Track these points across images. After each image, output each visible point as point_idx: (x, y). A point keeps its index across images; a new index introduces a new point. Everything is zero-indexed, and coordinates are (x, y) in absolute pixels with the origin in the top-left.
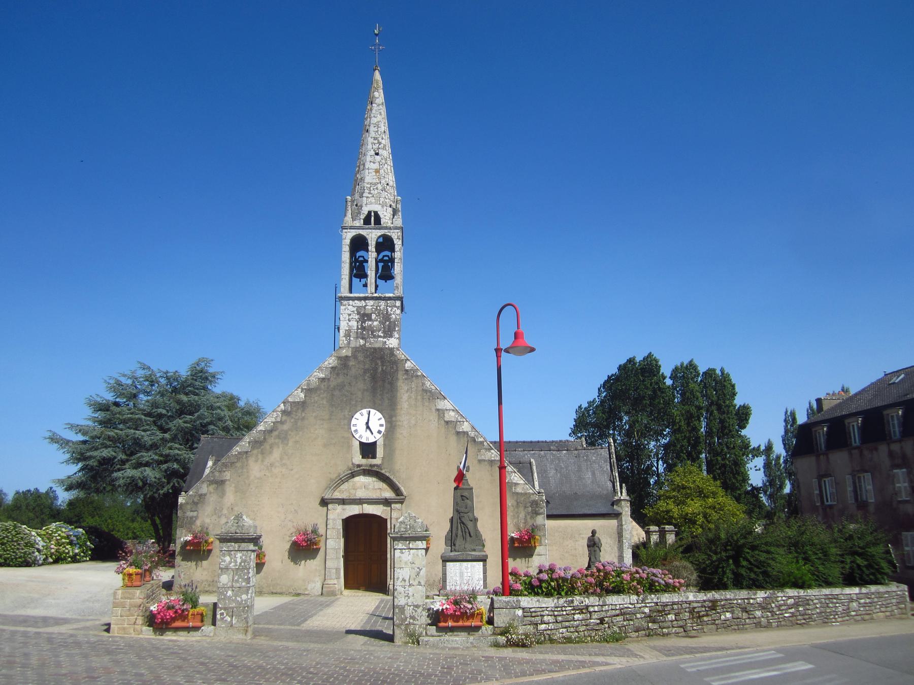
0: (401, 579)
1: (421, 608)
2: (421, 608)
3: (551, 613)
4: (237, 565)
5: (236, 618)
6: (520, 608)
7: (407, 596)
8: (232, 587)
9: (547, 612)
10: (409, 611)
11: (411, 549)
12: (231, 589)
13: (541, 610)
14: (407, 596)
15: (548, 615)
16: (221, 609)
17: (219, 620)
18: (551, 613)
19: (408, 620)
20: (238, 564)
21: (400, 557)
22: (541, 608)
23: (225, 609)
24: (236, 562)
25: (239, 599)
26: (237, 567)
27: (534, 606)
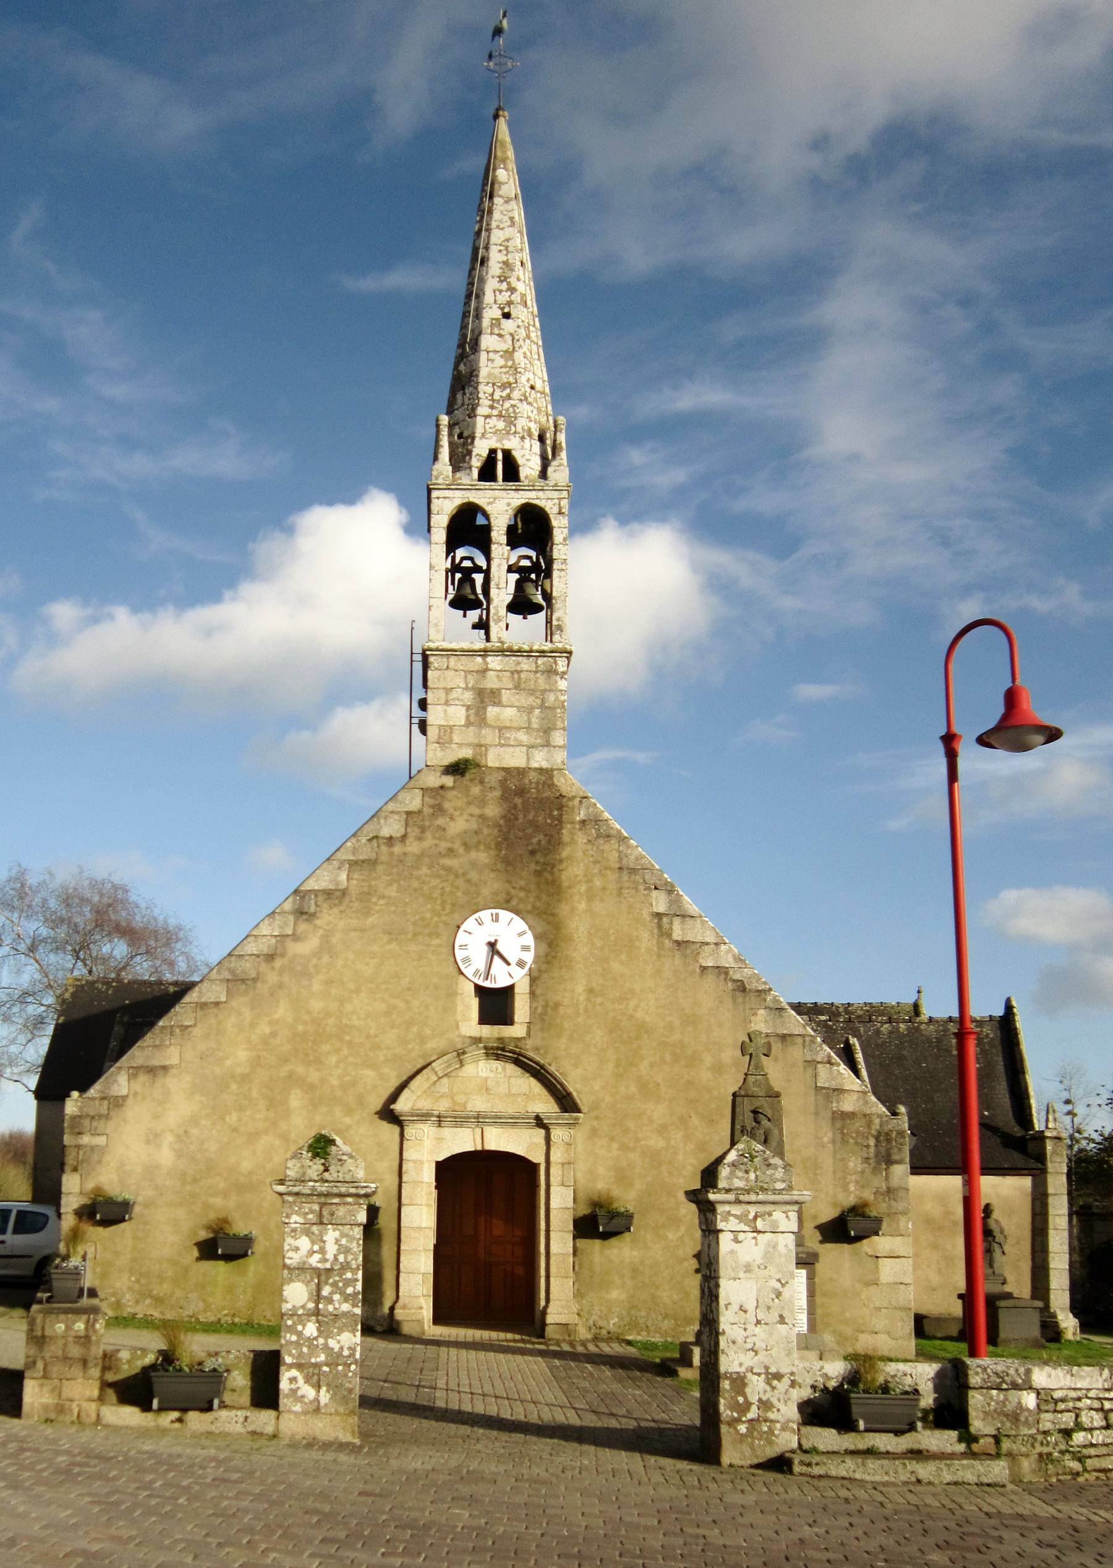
0: (735, 1307)
1: (786, 1381)
2: (786, 1381)
3: (1096, 1405)
4: (326, 1260)
5: (328, 1391)
6: (1030, 1388)
7: (752, 1349)
8: (317, 1313)
9: (1088, 1402)
10: (756, 1387)
11: (760, 1232)
12: (314, 1318)
13: (1073, 1394)
14: (752, 1349)
15: (1092, 1409)
16: (291, 1366)
17: (287, 1396)
18: (1096, 1405)
19: (754, 1408)
20: (330, 1256)
21: (732, 1252)
22: (1075, 1389)
23: (299, 1366)
24: (322, 1251)
25: (332, 1343)
26: (328, 1265)
27: (1062, 1384)
